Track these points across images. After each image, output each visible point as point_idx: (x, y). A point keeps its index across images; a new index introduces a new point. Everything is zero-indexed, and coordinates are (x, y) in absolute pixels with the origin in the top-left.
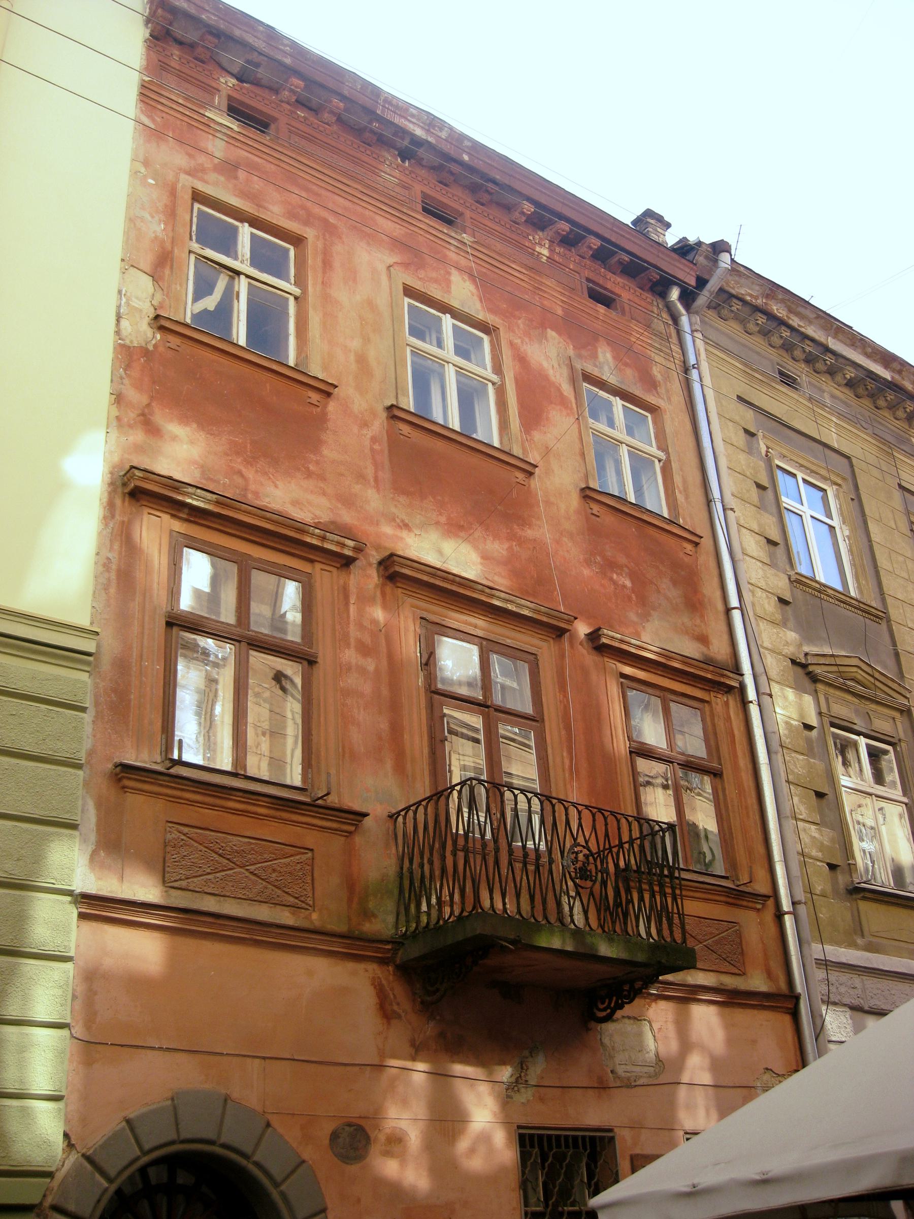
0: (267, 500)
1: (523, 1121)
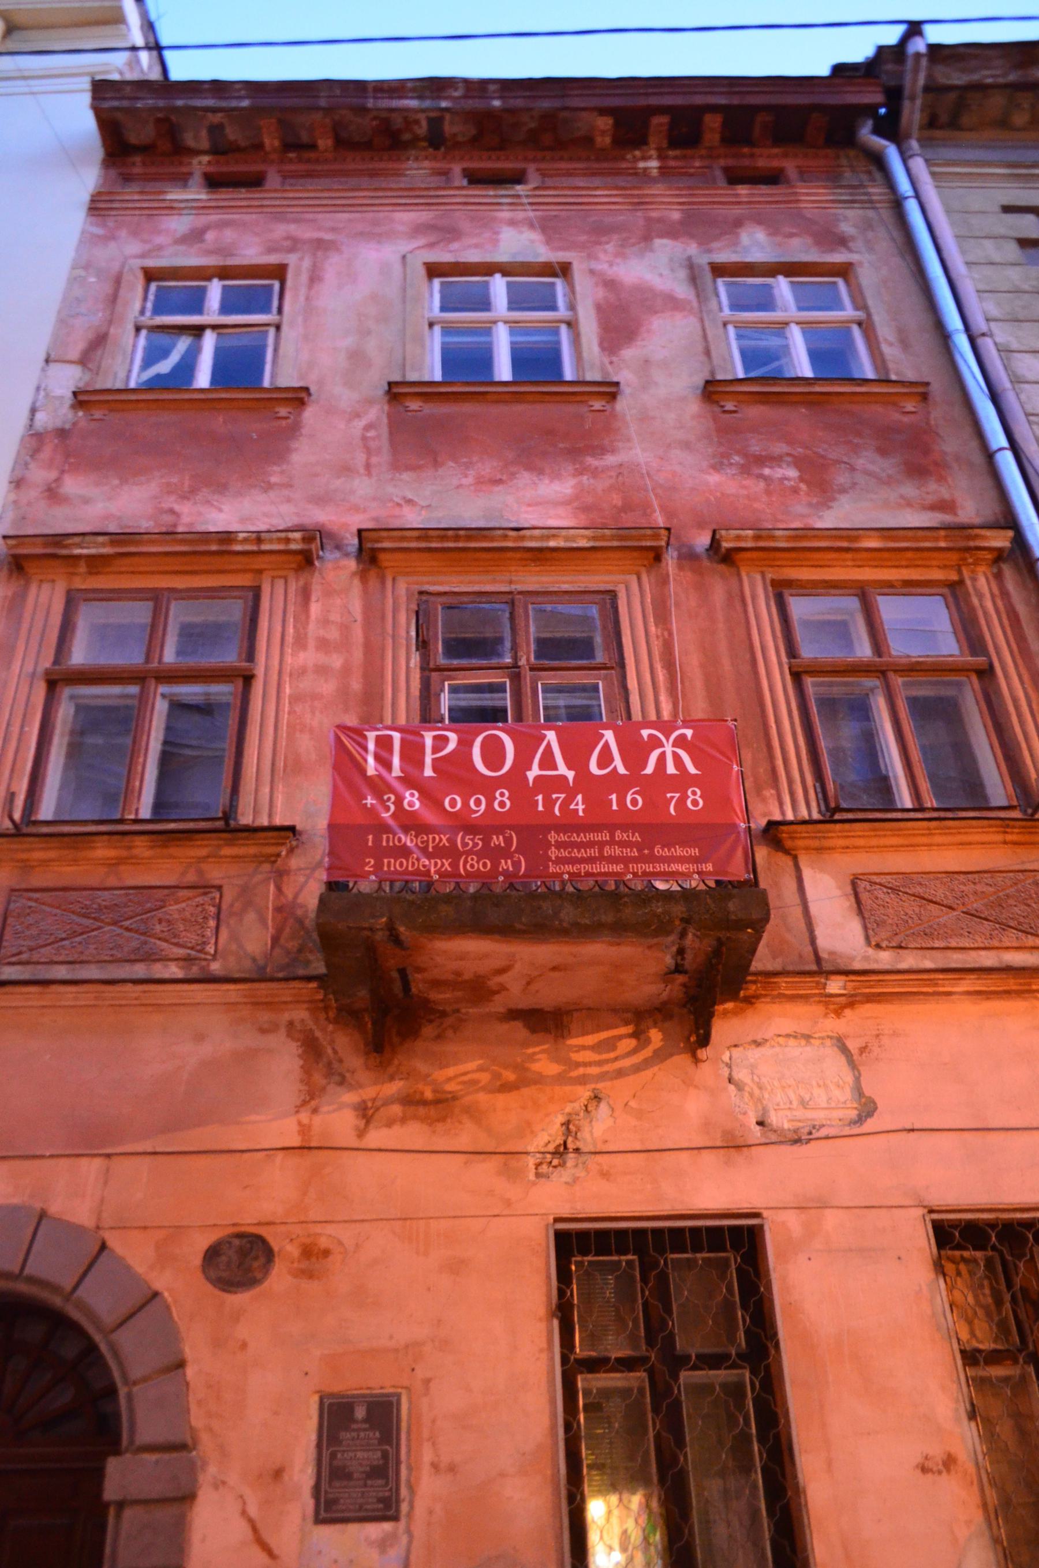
1: (565, 1212)
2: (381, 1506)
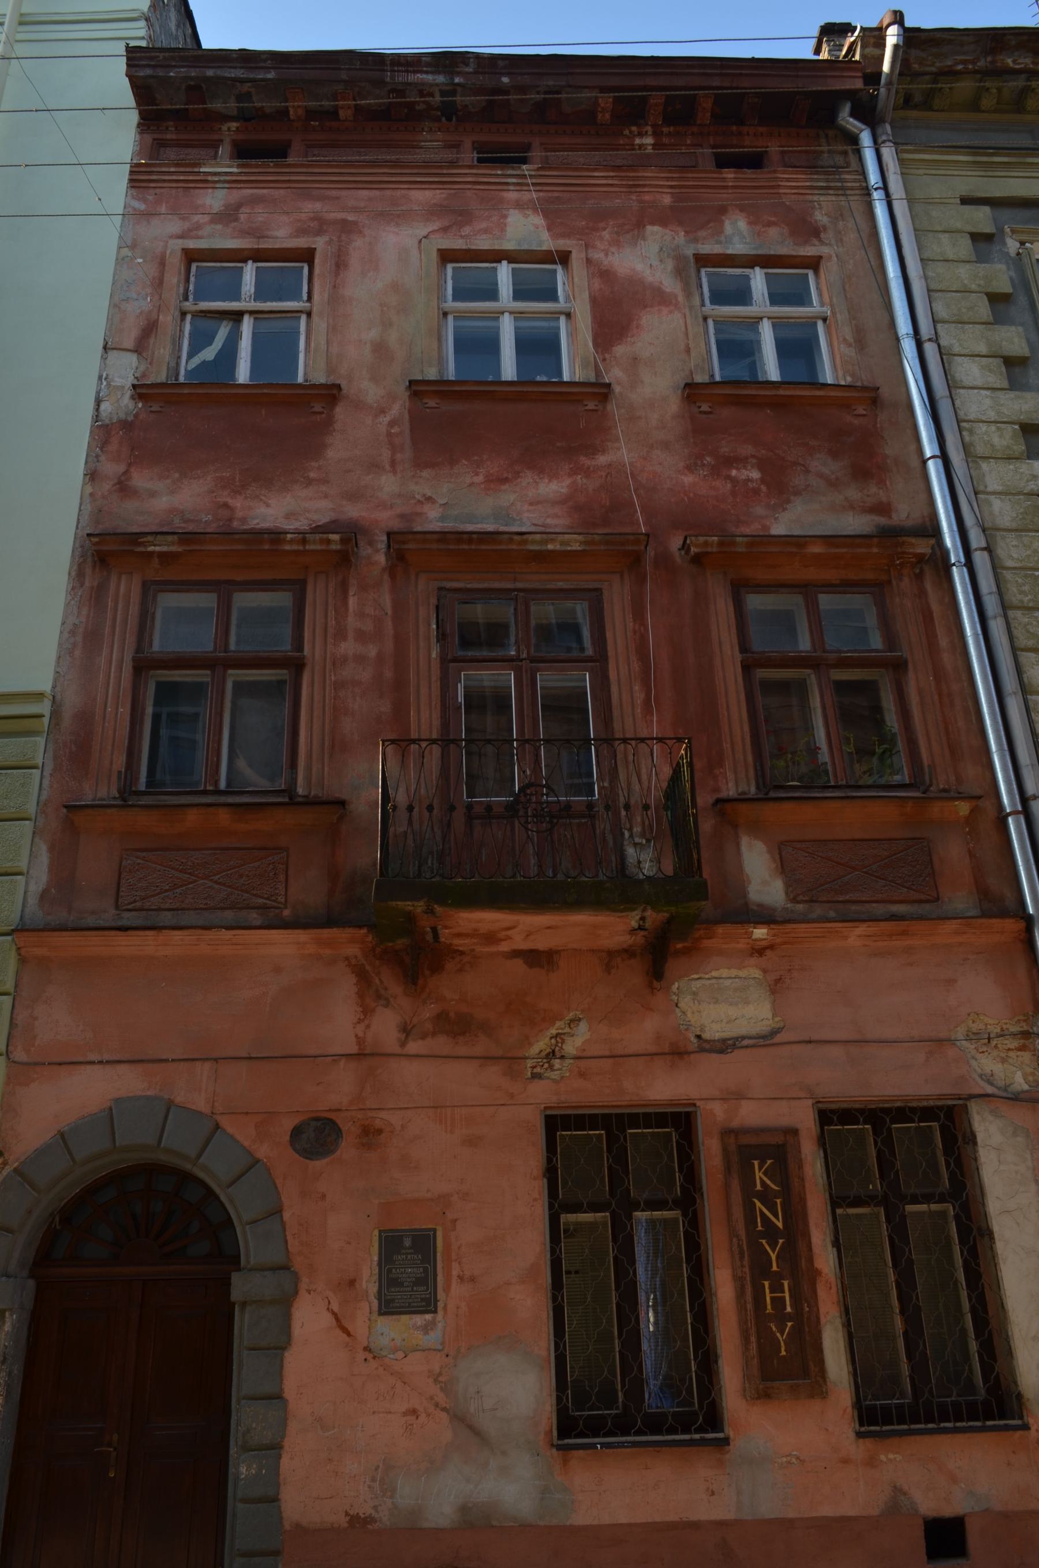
0: (256, 521)
2: (424, 1304)
